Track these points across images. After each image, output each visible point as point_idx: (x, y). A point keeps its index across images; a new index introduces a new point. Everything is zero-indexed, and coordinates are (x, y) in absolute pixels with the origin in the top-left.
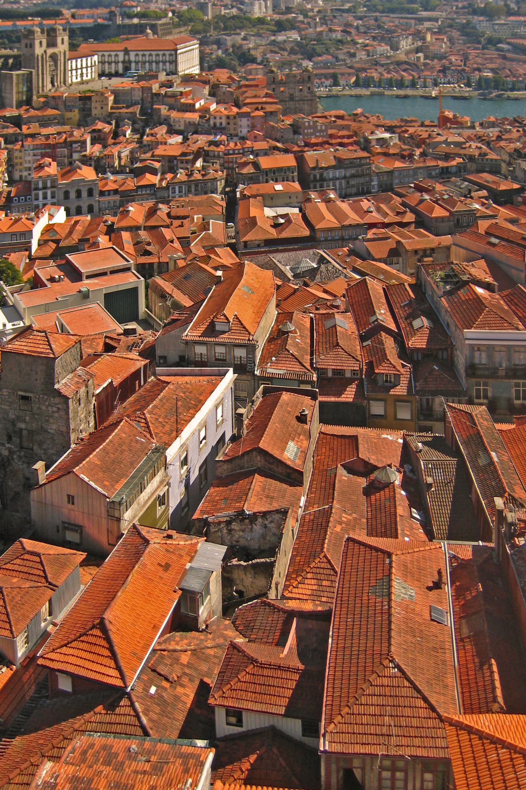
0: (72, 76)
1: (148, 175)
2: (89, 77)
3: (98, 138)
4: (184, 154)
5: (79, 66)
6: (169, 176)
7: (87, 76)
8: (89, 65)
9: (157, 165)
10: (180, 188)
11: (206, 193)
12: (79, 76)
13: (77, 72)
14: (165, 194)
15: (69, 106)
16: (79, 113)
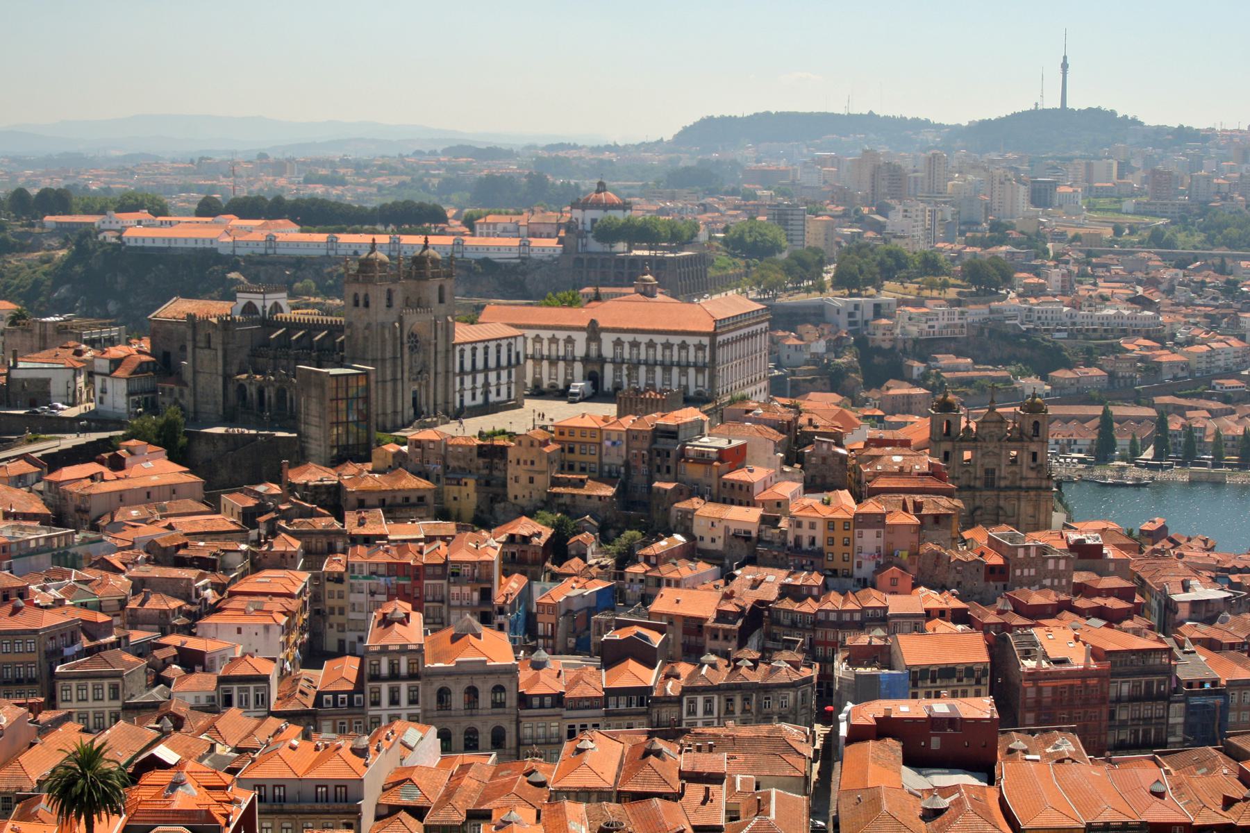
0: (462, 390)
1: (632, 664)
2: (504, 396)
3: (518, 558)
4: (722, 616)
5: (480, 364)
6: (684, 669)
7: (498, 394)
8: (504, 362)
9: (656, 639)
10: (708, 701)
11: (767, 719)
12: (478, 392)
13: (474, 381)
14: (667, 713)
15: (454, 470)
16: (477, 491)
